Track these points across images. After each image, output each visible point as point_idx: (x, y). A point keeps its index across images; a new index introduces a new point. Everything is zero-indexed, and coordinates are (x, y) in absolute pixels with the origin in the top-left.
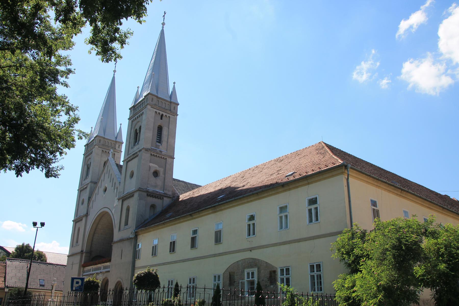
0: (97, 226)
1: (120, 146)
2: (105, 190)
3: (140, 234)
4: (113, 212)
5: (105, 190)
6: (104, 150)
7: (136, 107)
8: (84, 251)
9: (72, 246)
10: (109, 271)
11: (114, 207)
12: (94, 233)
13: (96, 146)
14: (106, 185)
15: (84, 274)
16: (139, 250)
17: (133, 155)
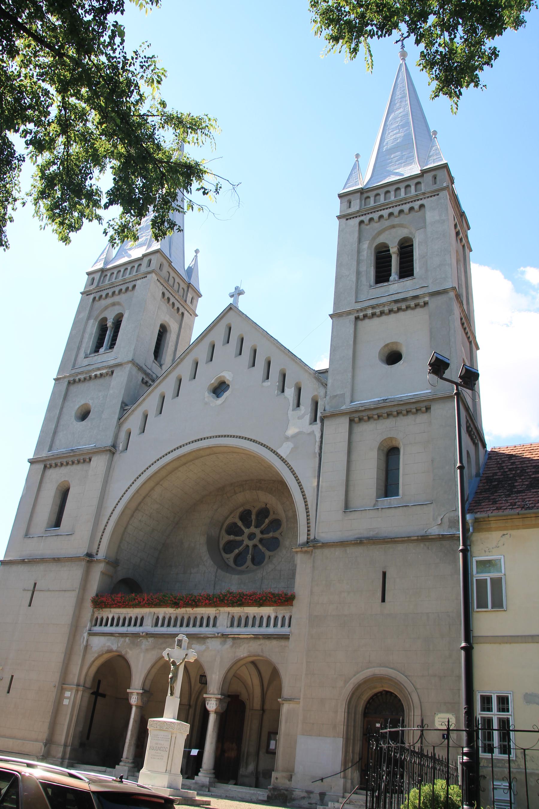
0: (153, 489)
1: (195, 301)
2: (219, 388)
3: (489, 530)
4: (284, 451)
5: (219, 388)
6: (167, 295)
7: (372, 194)
8: (101, 555)
9: (27, 535)
10: (285, 637)
11: (287, 439)
12: (137, 509)
13: (153, 275)
14: (228, 376)
15: (97, 629)
16: (497, 583)
17: (396, 301)
